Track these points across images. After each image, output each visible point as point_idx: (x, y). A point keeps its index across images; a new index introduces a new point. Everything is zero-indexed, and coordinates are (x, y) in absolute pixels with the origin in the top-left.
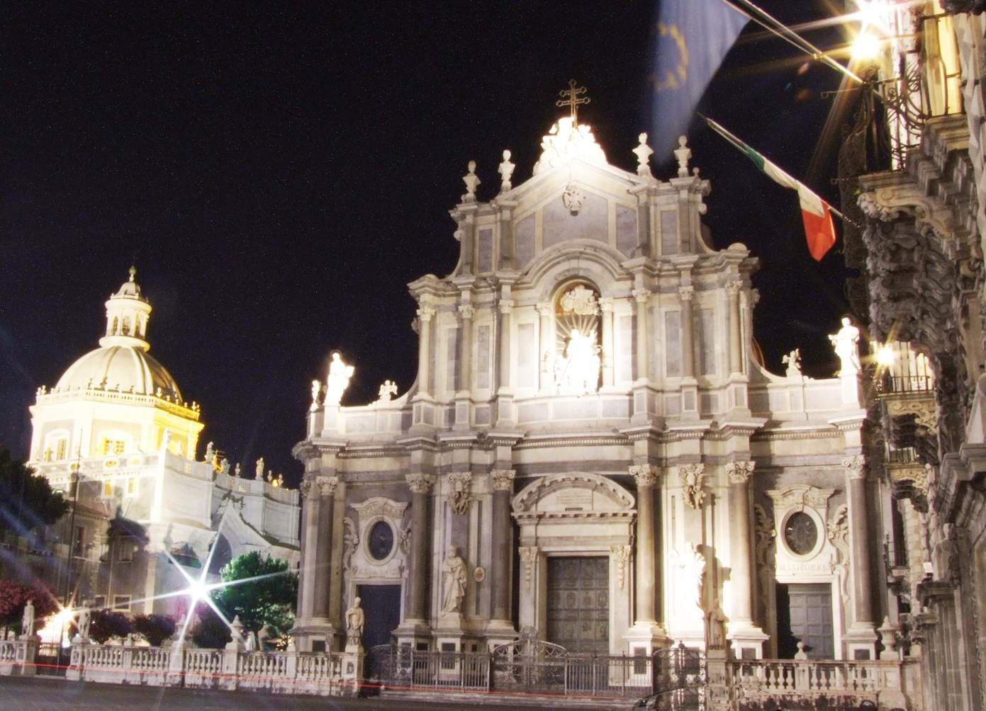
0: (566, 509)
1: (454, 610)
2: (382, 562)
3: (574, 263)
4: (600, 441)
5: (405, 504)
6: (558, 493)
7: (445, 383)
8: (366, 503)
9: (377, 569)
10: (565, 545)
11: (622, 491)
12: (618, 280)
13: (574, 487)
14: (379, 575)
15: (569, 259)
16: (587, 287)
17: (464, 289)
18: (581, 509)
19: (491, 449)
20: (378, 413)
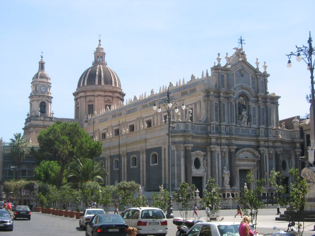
0: (245, 157)
1: (228, 184)
2: (199, 169)
3: (244, 90)
4: (251, 140)
5: (205, 153)
6: (243, 153)
7: (215, 119)
8: (195, 152)
9: (198, 172)
10: (245, 167)
11: (258, 154)
12: (253, 97)
13: (247, 152)
14: (198, 174)
15: (242, 89)
16: (242, 97)
17: (222, 93)
18: (248, 158)
19: (228, 140)
20: (197, 125)
